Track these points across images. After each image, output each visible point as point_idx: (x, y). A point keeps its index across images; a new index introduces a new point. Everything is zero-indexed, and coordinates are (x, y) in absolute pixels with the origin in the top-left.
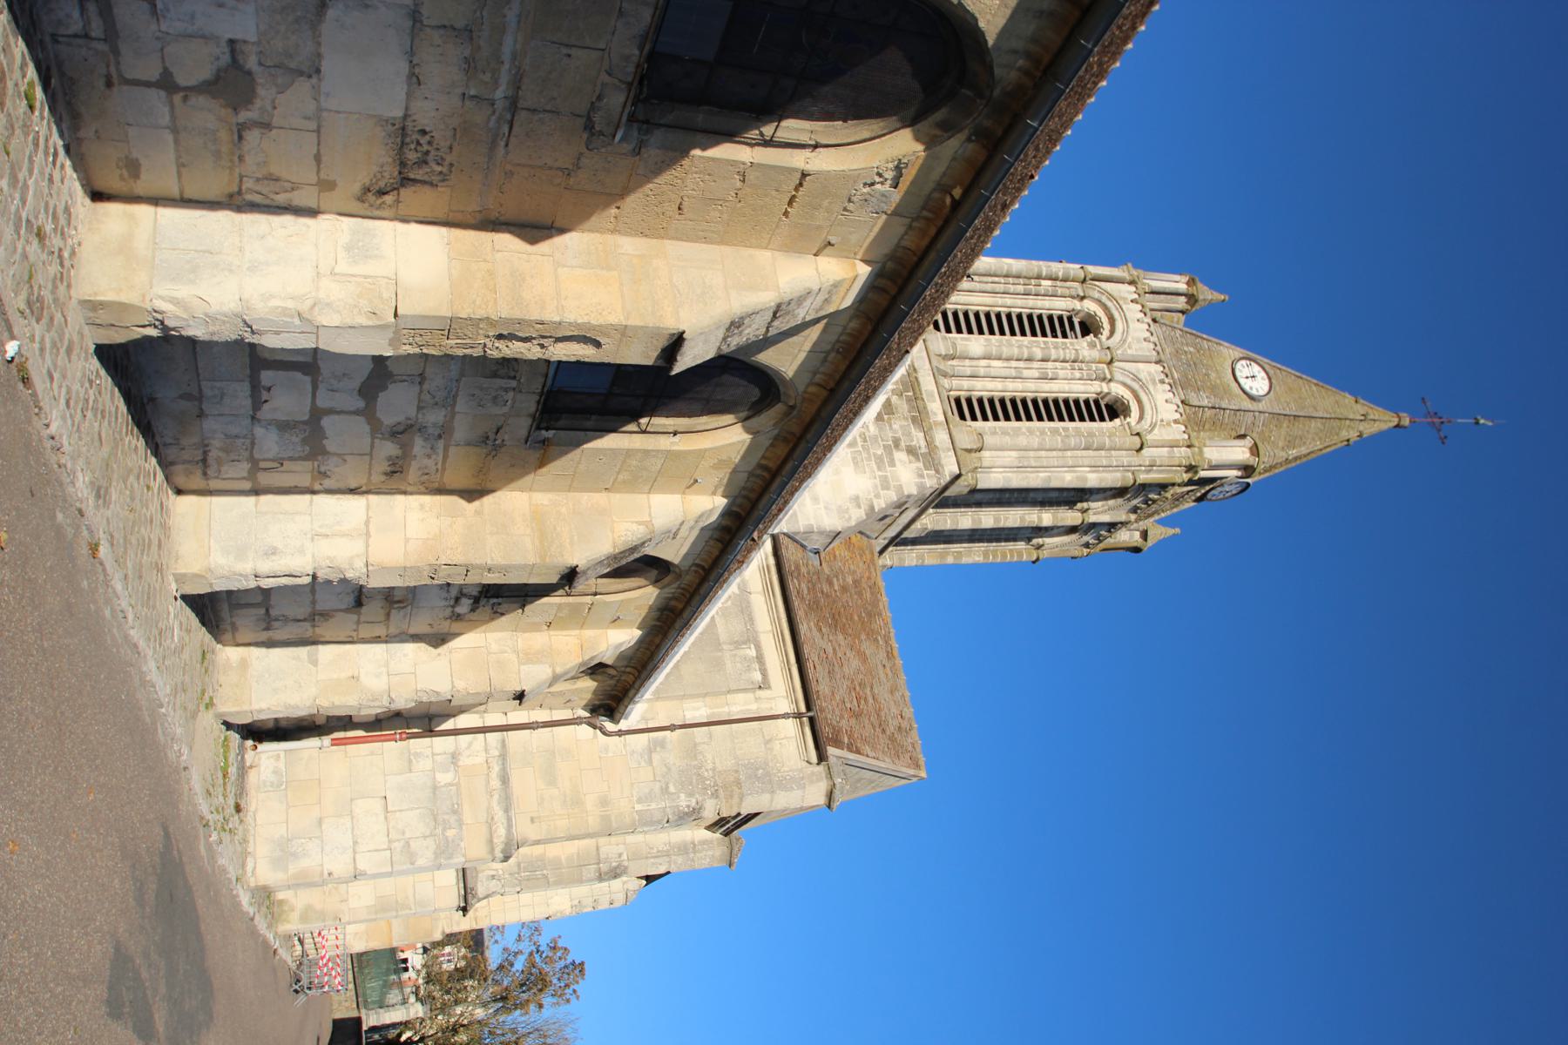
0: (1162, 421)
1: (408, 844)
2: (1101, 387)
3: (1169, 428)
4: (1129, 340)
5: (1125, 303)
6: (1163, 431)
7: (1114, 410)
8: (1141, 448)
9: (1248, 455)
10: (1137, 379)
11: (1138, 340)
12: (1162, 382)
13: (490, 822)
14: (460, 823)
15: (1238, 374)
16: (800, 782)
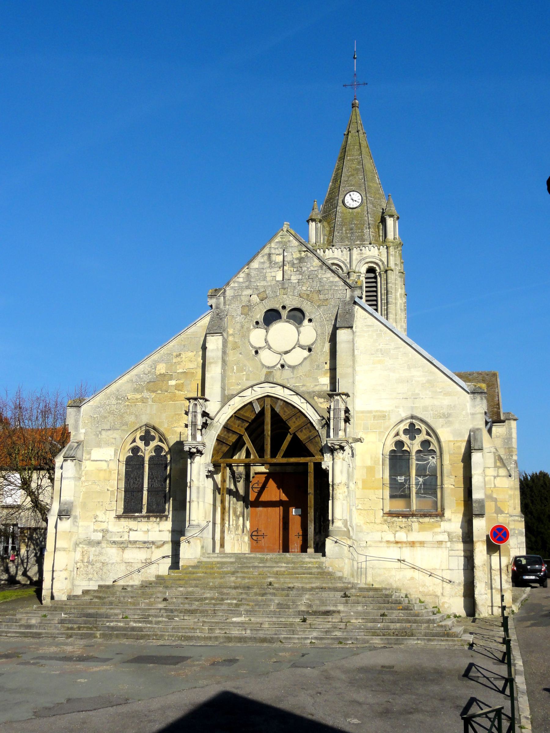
0: (379, 255)
1: (518, 543)
2: (362, 277)
3: (382, 253)
4: (342, 259)
5: (326, 256)
6: (383, 256)
7: (371, 270)
8: (392, 270)
9: (392, 219)
10: (360, 261)
11: (343, 255)
12: (361, 250)
13: (514, 521)
14: (514, 529)
15: (351, 206)
16: (510, 429)
